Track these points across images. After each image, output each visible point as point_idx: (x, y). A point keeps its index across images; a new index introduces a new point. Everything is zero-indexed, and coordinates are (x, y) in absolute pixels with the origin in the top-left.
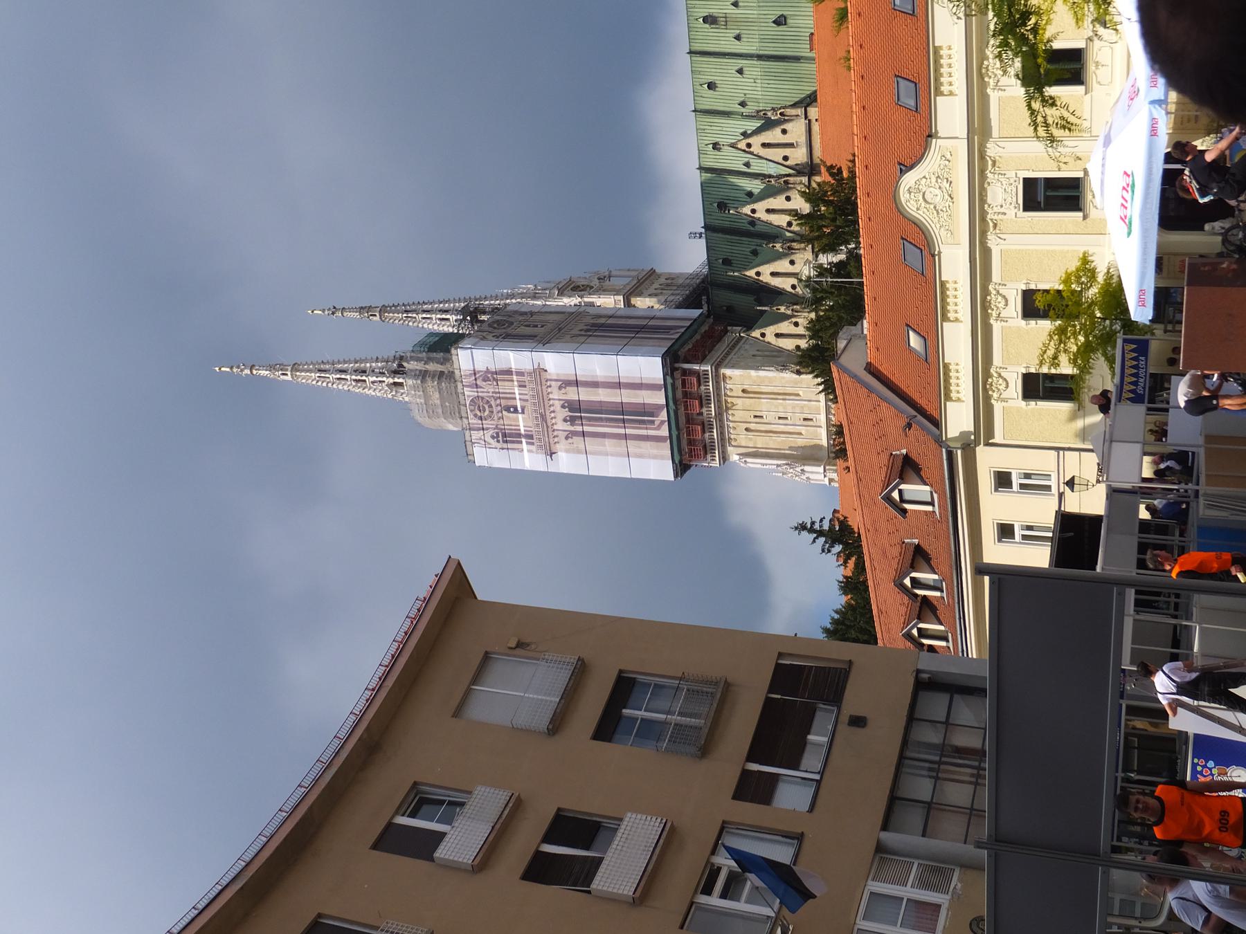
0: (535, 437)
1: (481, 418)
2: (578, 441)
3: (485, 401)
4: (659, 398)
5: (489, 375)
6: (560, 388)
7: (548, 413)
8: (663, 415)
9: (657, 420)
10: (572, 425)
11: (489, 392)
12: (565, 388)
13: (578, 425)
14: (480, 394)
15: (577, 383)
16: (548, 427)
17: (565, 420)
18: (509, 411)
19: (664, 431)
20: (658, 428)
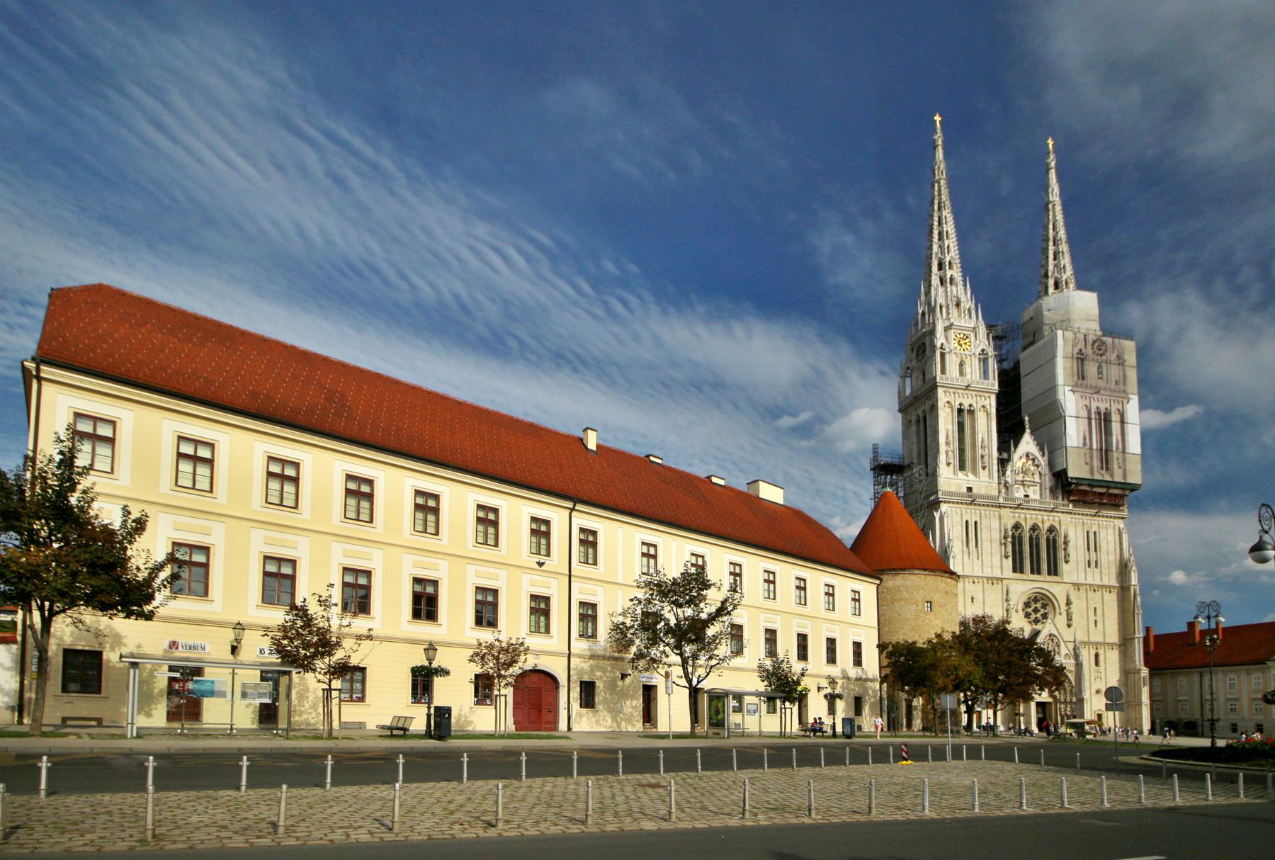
1: (1093, 345)
2: (1084, 413)
4: (1118, 478)
5: (1121, 361)
6: (1118, 410)
8: (1107, 478)
9: (1104, 472)
15: (1123, 422)
17: (1098, 408)
19: (1097, 477)
20: (1099, 473)
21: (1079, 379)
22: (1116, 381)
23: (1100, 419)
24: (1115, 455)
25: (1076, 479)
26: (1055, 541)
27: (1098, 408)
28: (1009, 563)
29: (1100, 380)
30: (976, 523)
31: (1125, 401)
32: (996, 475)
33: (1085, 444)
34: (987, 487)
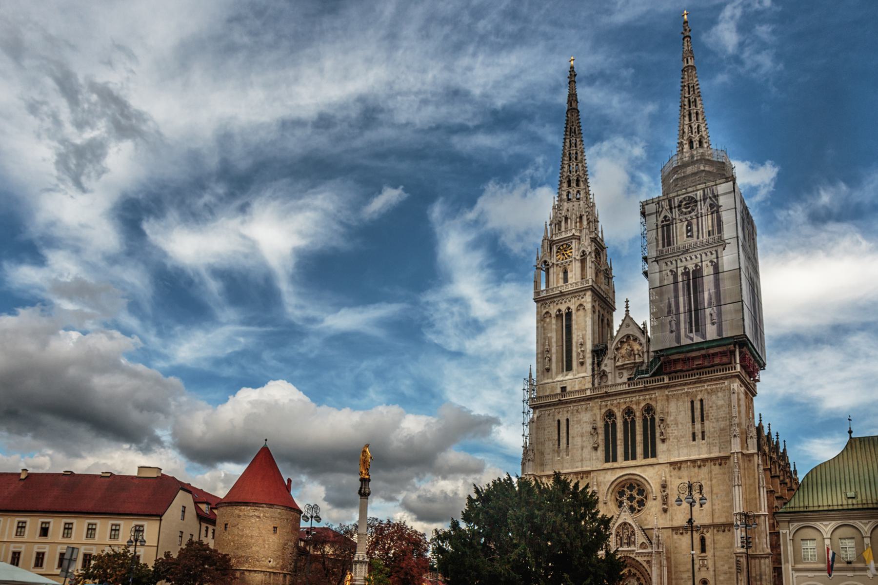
0: (669, 247)
1: (679, 206)
3: (694, 207)
5: (715, 208)
6: (711, 262)
7: (689, 255)
10: (682, 274)
11: (701, 210)
12: (712, 265)
13: (683, 278)
14: (699, 203)
16: (678, 256)
17: (685, 268)
18: (687, 226)
21: (664, 246)
22: (709, 232)
23: (689, 280)
24: (708, 311)
25: (661, 351)
26: (653, 419)
27: (685, 268)
28: (601, 453)
29: (689, 238)
30: (568, 420)
31: (720, 249)
32: (589, 368)
33: (669, 312)
34: (580, 383)
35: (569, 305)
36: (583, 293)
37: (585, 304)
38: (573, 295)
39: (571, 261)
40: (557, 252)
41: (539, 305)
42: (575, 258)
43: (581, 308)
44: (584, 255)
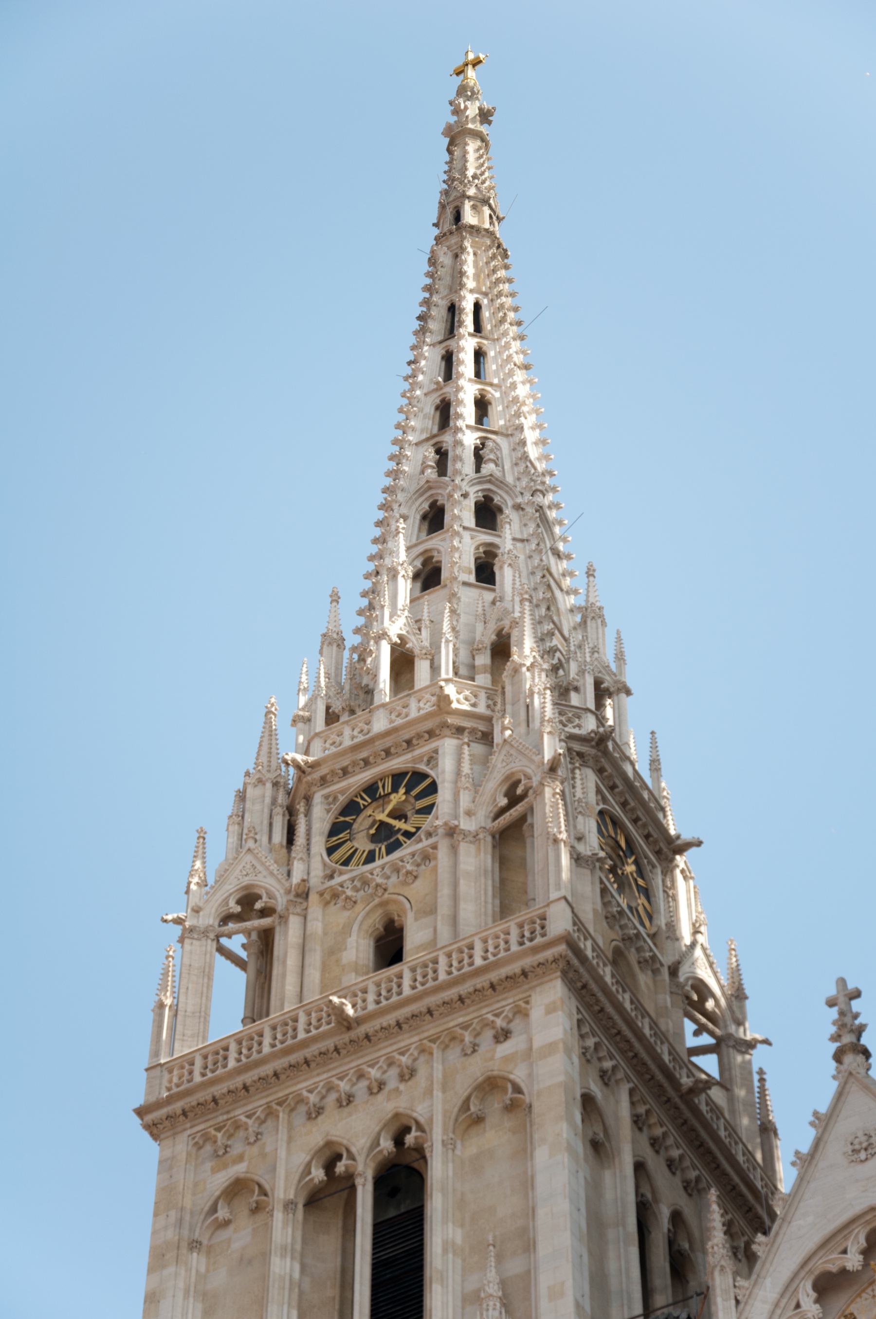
35: (401, 1104)
36: (507, 1001)
37: (519, 1074)
38: (431, 1029)
39: (427, 857)
40: (335, 829)
41: (182, 1145)
42: (452, 832)
43: (495, 1104)
44: (514, 800)
